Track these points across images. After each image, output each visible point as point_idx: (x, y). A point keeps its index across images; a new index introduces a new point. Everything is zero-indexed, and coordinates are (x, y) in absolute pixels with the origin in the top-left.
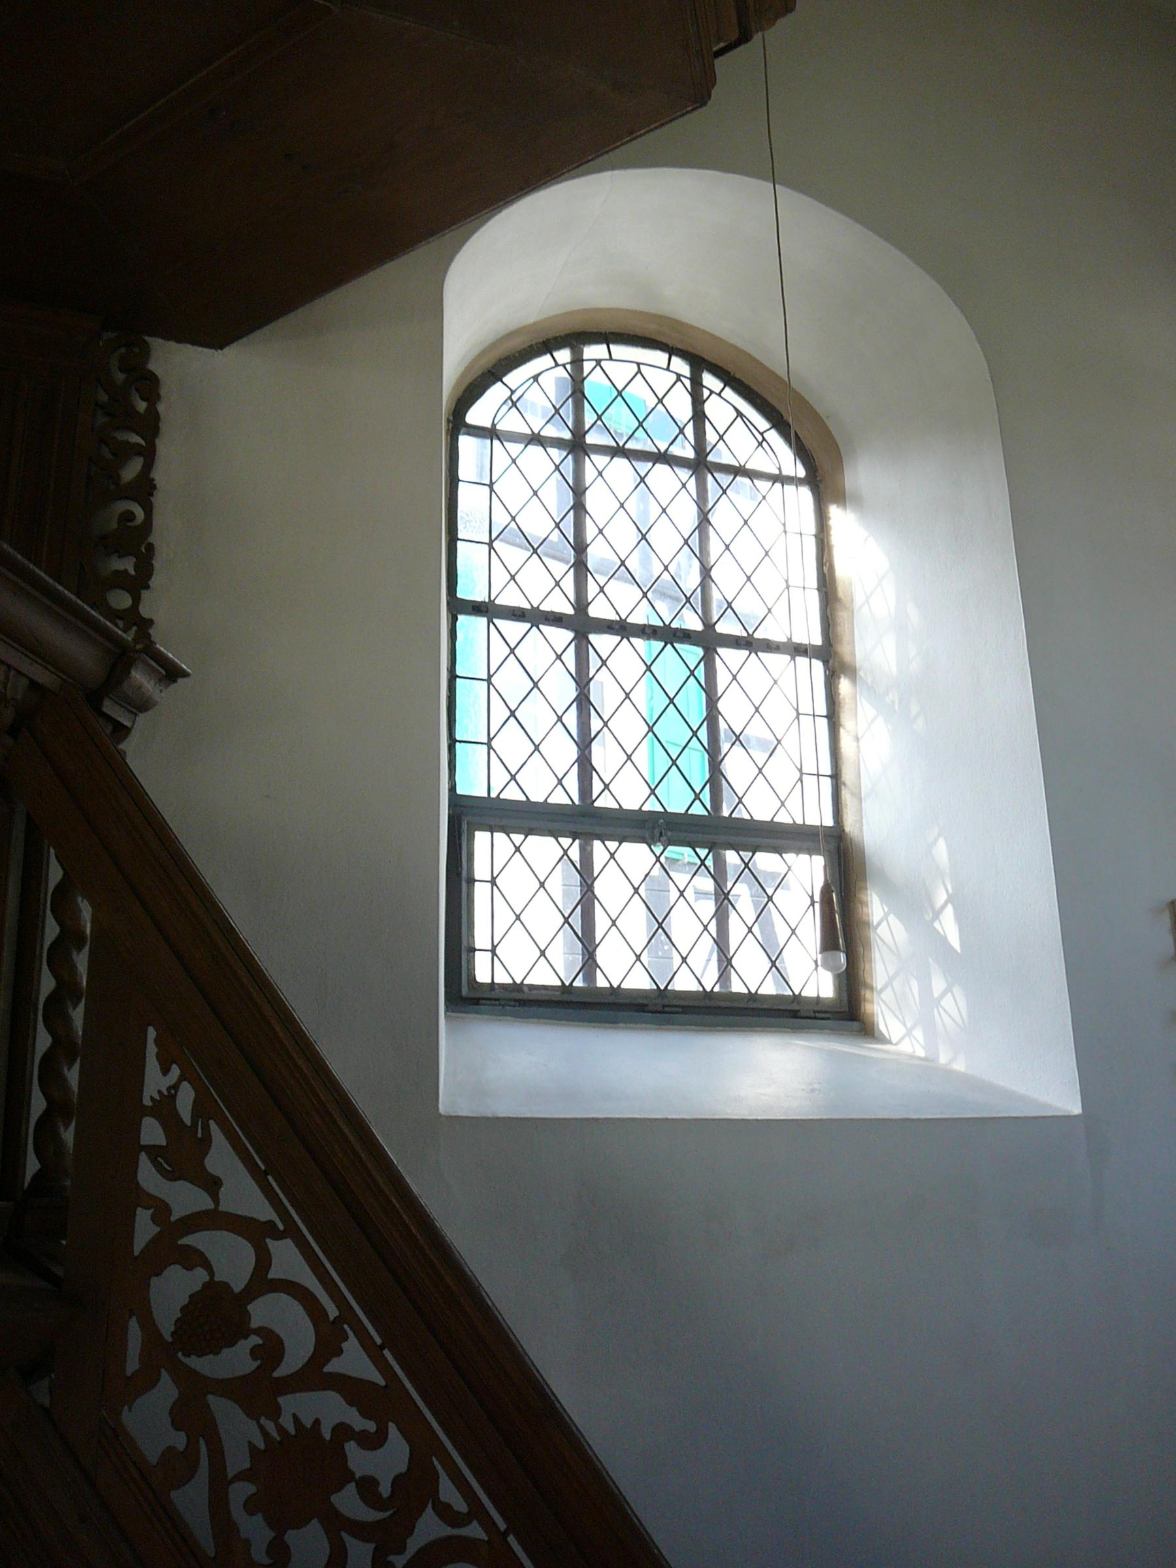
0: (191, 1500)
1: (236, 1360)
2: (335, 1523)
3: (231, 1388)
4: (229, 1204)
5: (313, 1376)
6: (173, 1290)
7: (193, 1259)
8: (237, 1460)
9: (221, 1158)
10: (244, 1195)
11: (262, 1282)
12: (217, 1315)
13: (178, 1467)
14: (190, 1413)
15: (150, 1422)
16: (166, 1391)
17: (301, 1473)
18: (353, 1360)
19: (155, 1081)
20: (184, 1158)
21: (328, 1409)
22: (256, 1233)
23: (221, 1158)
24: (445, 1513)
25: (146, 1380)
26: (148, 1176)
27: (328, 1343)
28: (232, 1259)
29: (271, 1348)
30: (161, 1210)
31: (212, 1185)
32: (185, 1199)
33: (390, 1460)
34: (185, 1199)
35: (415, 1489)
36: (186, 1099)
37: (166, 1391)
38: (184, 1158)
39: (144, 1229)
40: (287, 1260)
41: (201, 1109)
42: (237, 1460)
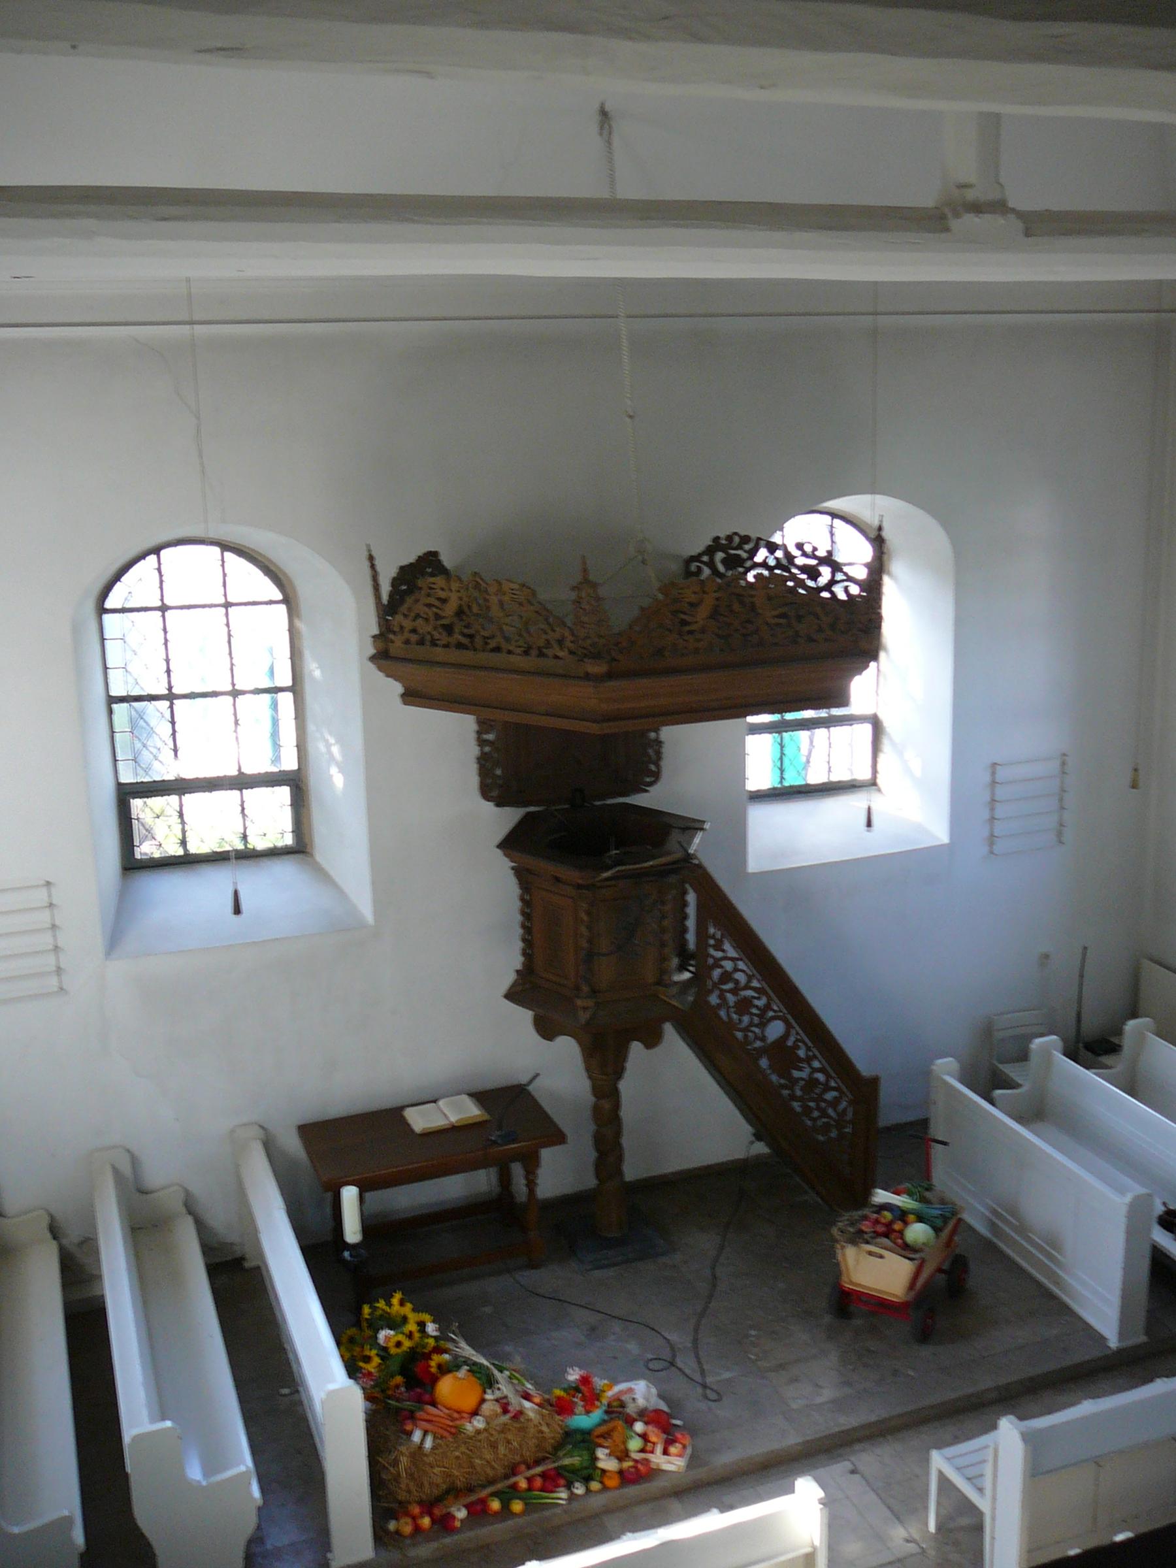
0: (723, 1013)
1: (730, 986)
2: (752, 1014)
3: (729, 991)
4: (730, 955)
5: (747, 987)
6: (716, 973)
7: (722, 967)
8: (731, 1004)
9: (727, 946)
10: (732, 953)
11: (736, 970)
12: (726, 977)
13: (719, 1006)
14: (722, 997)
15: (714, 999)
16: (717, 993)
17: (744, 1006)
18: (755, 984)
19: (712, 930)
20: (718, 947)
21: (750, 993)
22: (732, 959)
23: (727, 946)
24: (775, 1011)
25: (711, 992)
26: (712, 951)
27: (749, 981)
28: (728, 966)
29: (737, 982)
30: (712, 957)
31: (723, 951)
32: (719, 954)
33: (761, 1003)
34: (719, 954)
35: (768, 1007)
36: (718, 935)
37: (717, 993)
38: (718, 947)
39: (711, 961)
40: (741, 965)
41: (722, 935)
42: (731, 1004)
